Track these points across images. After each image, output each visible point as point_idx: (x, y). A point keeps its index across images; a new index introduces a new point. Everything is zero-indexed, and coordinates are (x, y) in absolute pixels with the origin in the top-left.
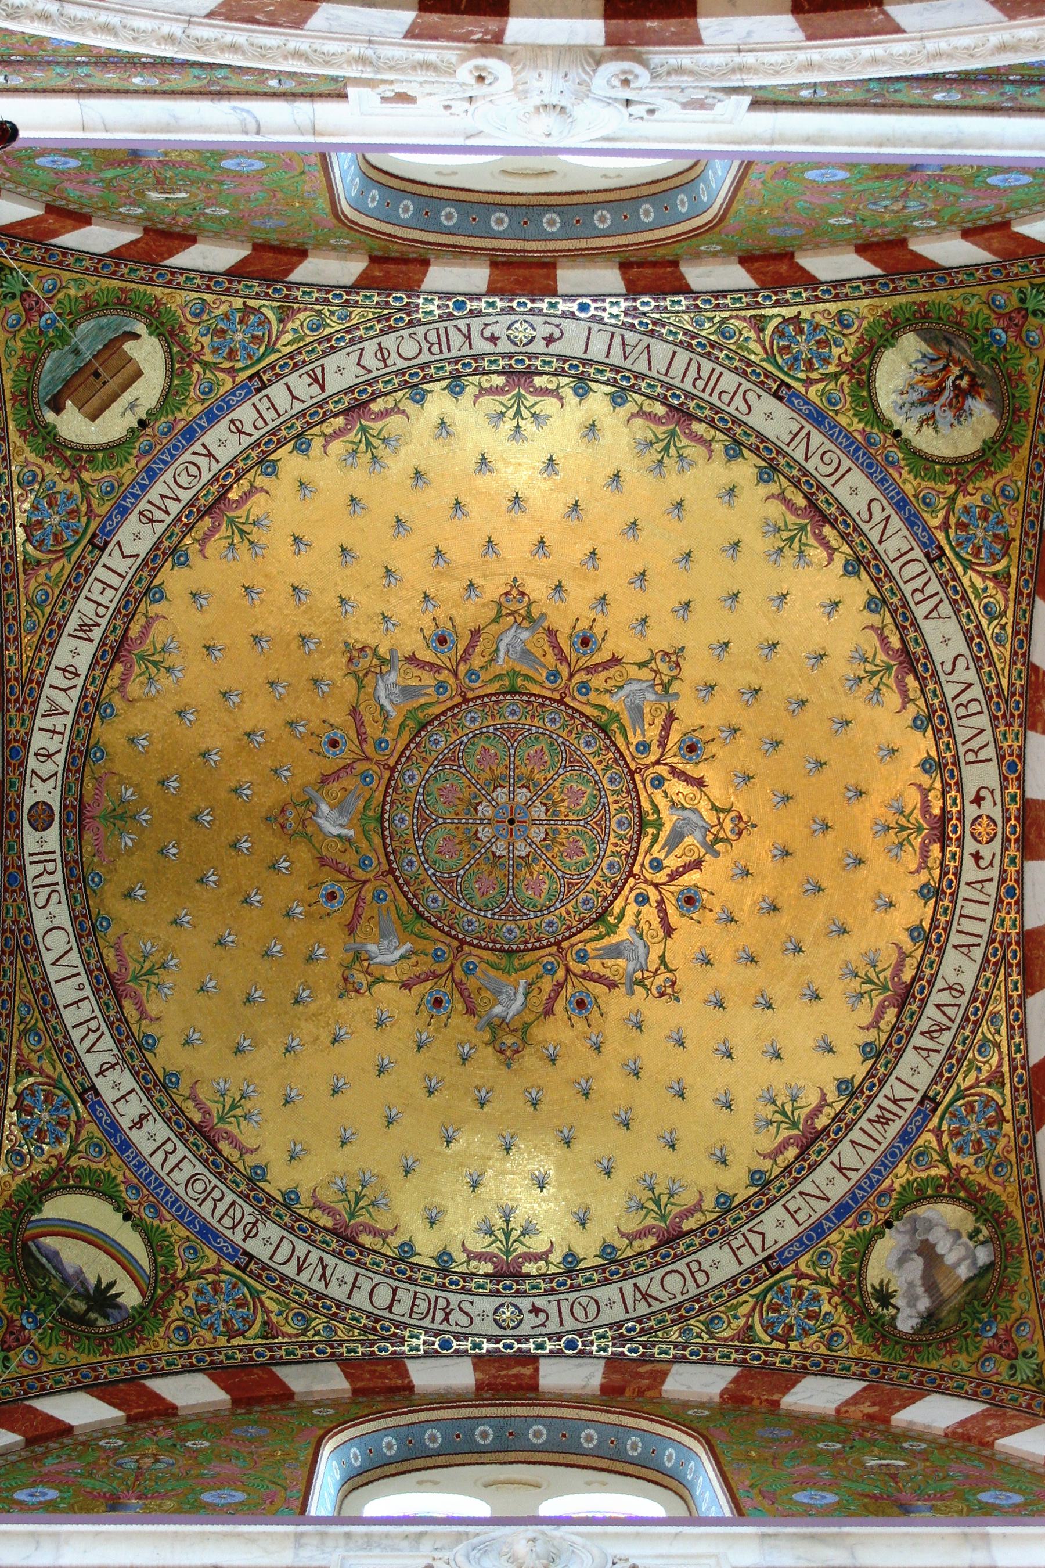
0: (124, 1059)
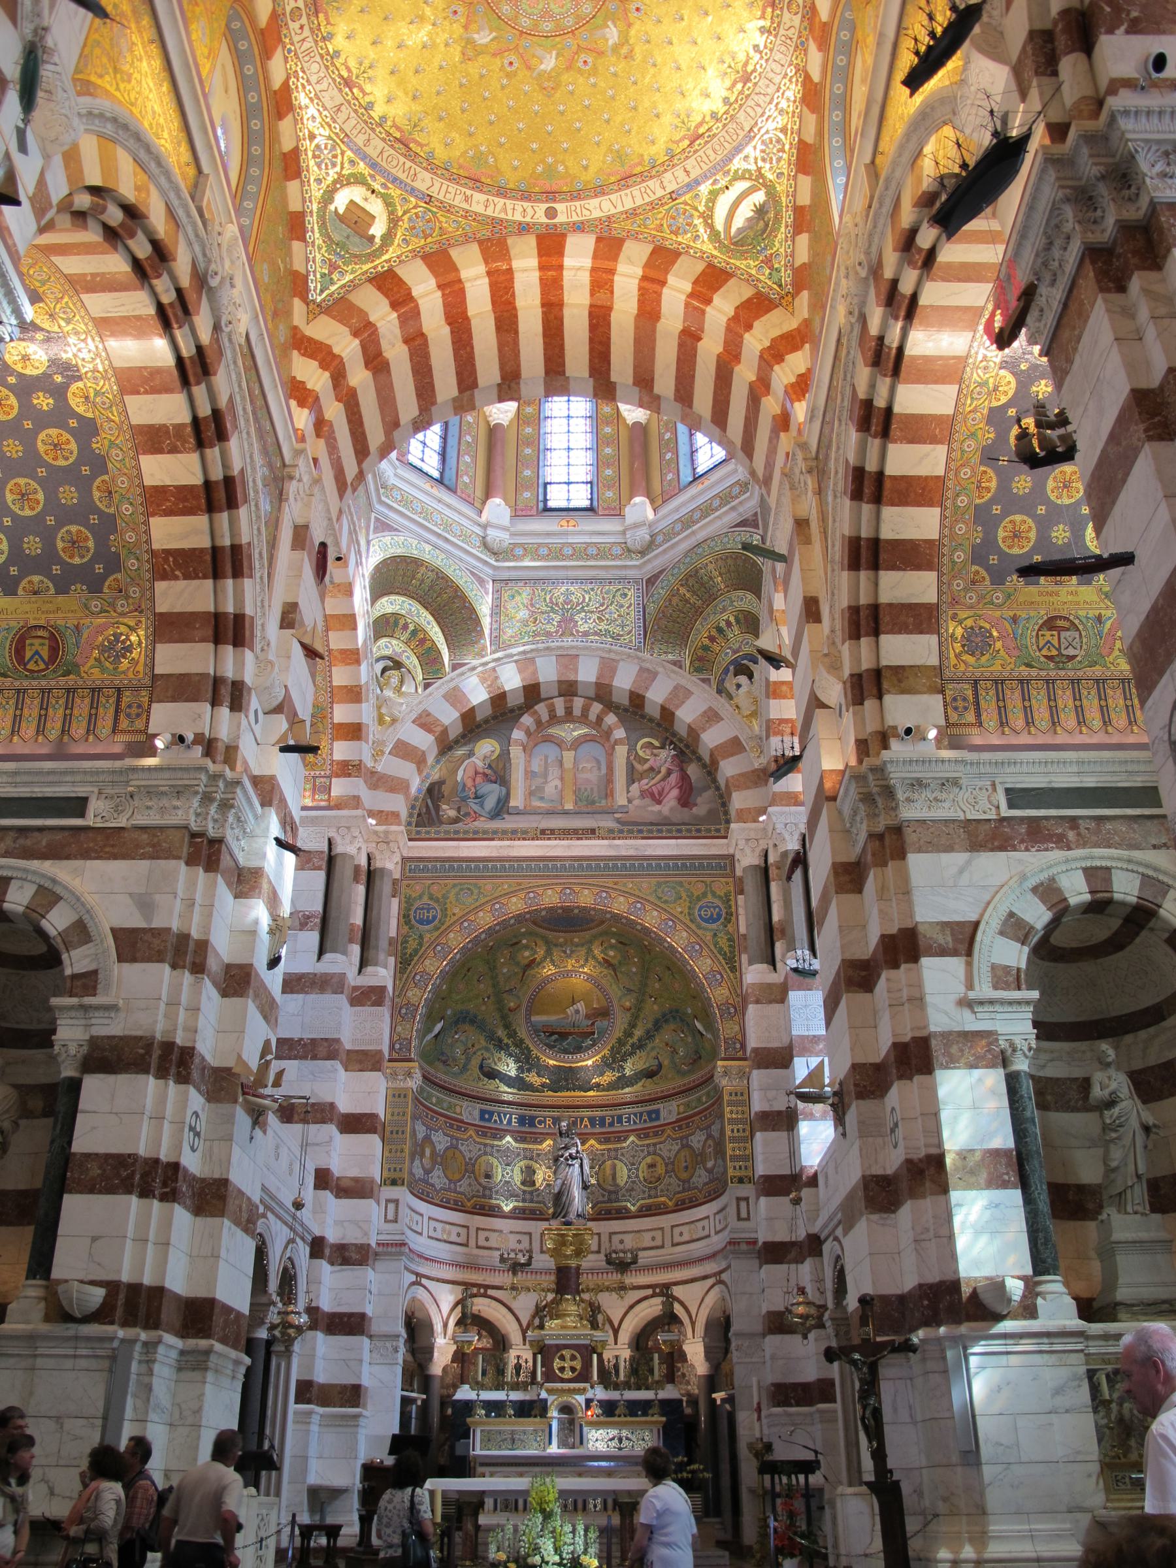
0: (659, 175)
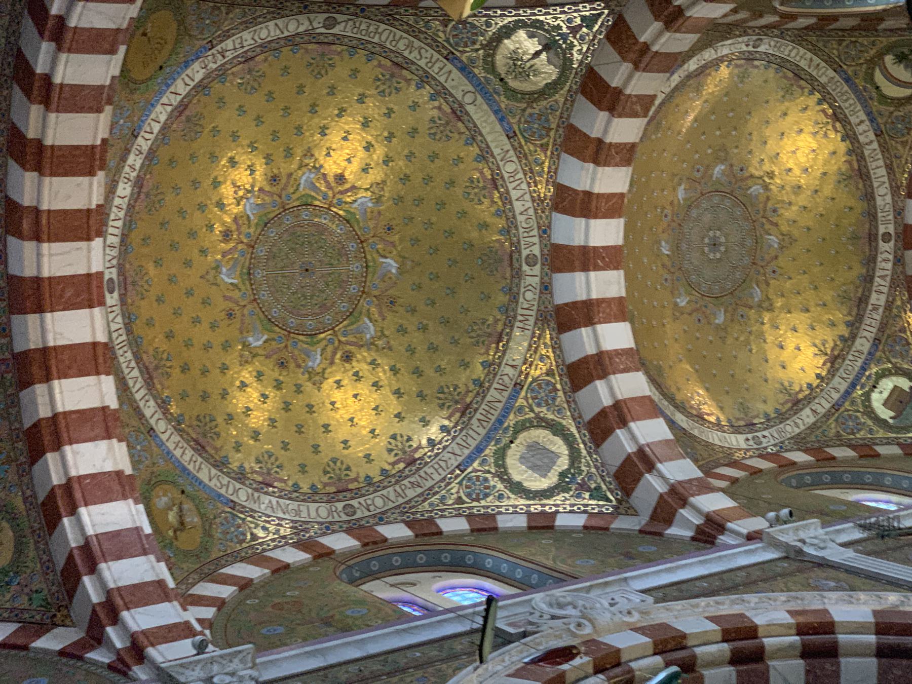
0: (861, 146)
